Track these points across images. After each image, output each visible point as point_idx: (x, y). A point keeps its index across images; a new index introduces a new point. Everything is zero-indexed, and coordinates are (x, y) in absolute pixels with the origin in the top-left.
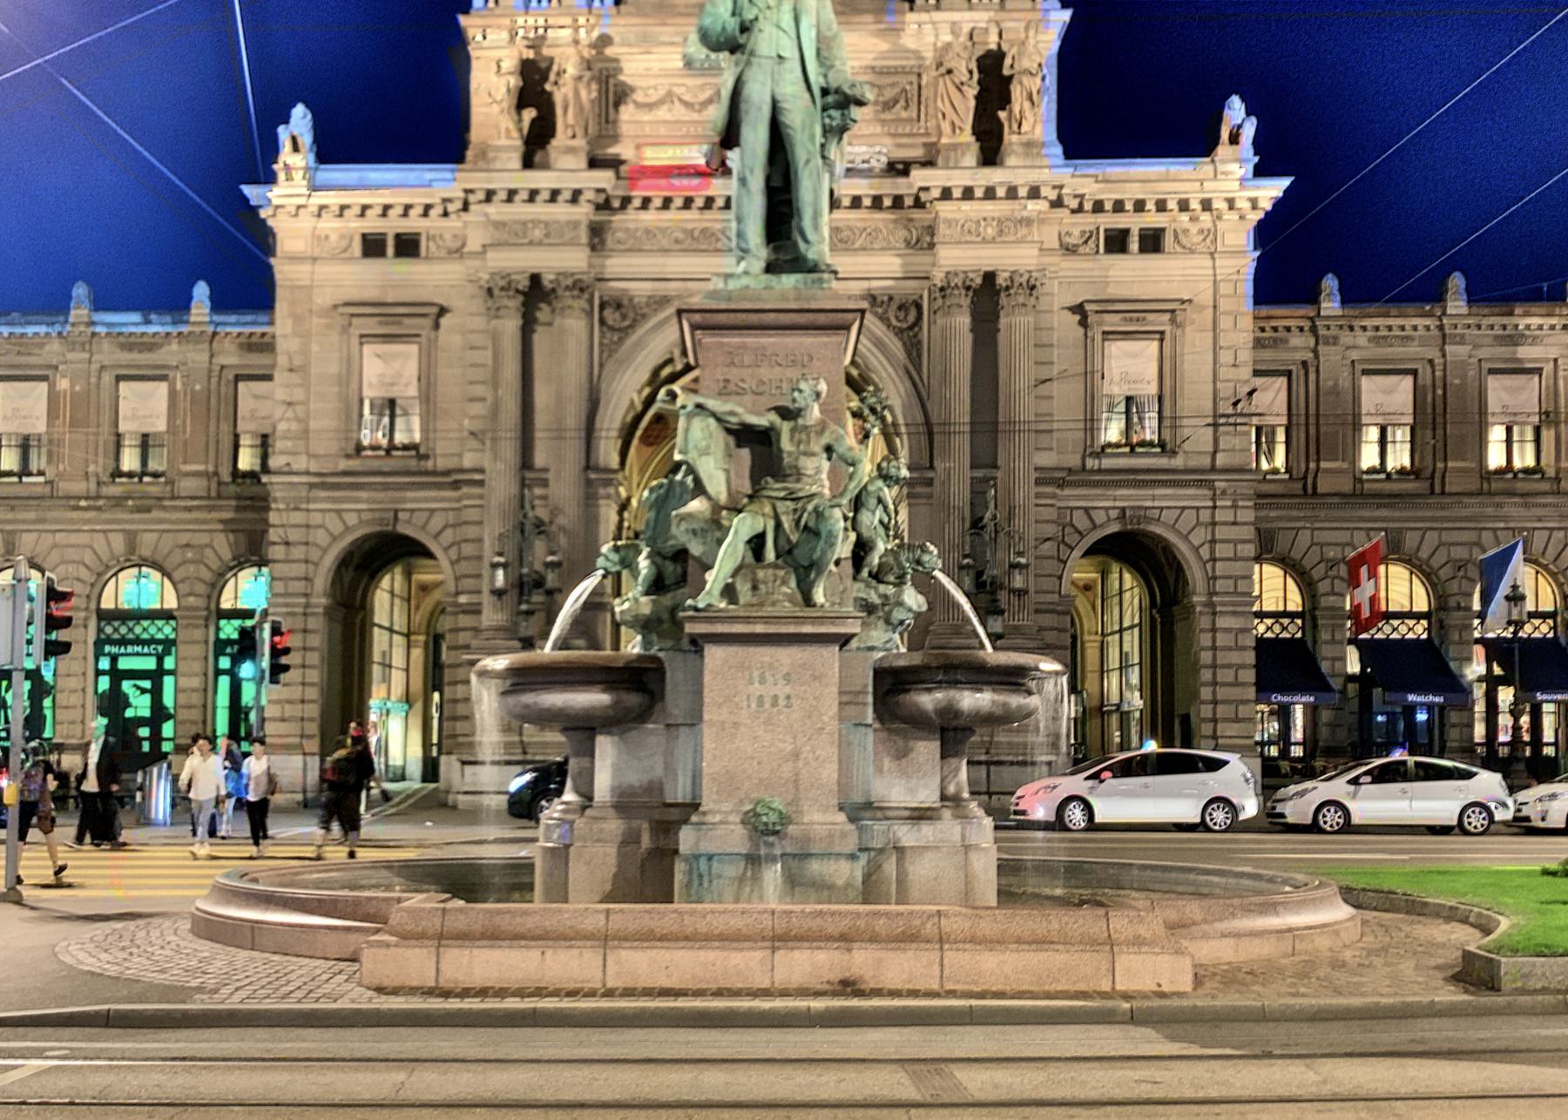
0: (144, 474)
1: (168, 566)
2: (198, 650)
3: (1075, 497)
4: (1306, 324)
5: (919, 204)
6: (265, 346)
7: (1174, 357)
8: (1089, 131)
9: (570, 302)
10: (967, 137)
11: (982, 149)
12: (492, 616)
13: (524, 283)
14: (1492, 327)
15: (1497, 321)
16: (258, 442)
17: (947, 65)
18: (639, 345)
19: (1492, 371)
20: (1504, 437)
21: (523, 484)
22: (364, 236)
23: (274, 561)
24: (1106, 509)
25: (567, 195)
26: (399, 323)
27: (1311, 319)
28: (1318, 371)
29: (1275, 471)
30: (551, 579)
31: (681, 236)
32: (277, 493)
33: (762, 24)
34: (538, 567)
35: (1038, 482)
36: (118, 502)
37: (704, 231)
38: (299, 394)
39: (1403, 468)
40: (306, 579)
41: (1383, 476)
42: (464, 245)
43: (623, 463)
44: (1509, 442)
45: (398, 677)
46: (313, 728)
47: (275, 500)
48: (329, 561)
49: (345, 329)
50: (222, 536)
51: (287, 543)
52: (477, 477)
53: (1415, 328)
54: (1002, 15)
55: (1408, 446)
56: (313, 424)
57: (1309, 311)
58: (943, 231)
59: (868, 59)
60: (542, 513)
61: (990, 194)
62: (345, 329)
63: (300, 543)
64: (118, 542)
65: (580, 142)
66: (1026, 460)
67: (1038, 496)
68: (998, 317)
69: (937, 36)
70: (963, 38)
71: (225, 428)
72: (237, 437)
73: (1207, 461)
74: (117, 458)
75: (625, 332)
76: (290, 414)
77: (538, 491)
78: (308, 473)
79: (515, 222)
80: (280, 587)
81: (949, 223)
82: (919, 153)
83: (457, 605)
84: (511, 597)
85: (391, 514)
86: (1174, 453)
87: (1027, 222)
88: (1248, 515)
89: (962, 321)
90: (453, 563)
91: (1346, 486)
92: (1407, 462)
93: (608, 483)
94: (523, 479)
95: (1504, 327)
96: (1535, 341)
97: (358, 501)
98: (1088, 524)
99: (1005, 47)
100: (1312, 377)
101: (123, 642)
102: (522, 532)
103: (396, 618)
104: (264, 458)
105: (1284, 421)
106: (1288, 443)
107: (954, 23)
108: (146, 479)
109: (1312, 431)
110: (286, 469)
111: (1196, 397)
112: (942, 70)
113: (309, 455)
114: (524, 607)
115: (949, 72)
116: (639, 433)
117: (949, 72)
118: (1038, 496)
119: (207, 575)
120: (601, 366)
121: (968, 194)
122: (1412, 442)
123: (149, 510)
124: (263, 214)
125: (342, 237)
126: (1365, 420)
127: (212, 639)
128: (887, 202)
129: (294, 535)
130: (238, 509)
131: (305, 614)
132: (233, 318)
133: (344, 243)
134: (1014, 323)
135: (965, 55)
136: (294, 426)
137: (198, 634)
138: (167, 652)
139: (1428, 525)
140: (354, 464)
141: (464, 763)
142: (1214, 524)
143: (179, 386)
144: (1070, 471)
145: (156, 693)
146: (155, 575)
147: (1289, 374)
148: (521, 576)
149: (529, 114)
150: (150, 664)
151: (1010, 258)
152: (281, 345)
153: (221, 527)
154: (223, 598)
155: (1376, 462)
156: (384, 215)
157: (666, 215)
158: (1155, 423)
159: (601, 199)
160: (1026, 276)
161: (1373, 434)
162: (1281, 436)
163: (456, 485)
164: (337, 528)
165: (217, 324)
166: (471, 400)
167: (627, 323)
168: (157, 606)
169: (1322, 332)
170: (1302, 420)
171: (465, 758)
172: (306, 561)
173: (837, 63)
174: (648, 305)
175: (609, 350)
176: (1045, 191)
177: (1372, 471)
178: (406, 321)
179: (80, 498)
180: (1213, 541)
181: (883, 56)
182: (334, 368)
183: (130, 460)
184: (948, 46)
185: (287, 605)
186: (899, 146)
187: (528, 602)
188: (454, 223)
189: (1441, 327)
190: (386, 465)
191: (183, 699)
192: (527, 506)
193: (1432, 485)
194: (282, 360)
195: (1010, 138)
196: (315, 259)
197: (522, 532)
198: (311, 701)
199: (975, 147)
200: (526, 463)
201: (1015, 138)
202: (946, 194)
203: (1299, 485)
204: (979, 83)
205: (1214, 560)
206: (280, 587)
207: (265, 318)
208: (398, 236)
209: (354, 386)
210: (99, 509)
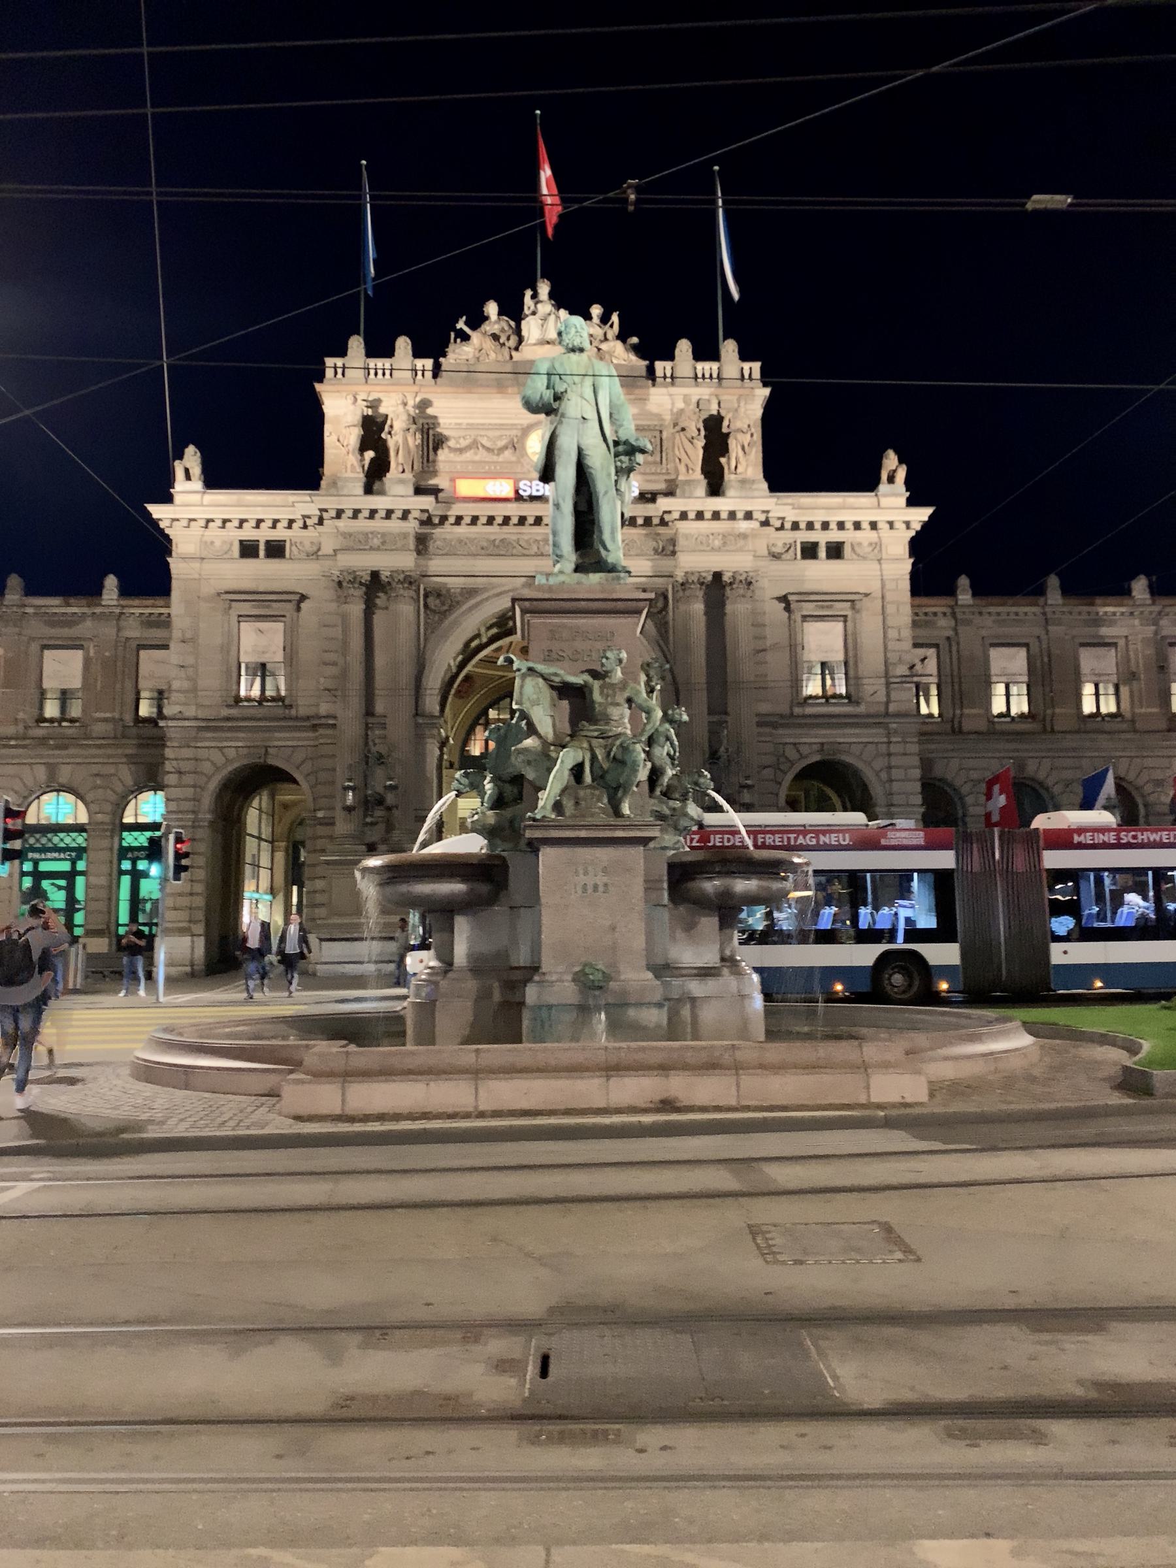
0: (63, 719)
1: (81, 791)
2: (105, 855)
3: (787, 735)
4: (948, 610)
5: (663, 523)
6: (164, 623)
7: (855, 634)
8: (784, 474)
9: (402, 592)
10: (698, 475)
11: (710, 485)
12: (343, 826)
13: (366, 578)
14: (1080, 613)
15: (1085, 609)
16: (156, 695)
17: (682, 425)
18: (456, 623)
19: (1083, 645)
20: (1093, 691)
21: (367, 727)
22: (241, 541)
23: (167, 786)
24: (810, 745)
25: (399, 514)
26: (268, 607)
27: (952, 607)
28: (958, 644)
29: (930, 716)
30: (390, 799)
31: (485, 544)
32: (171, 734)
33: (570, 395)
34: (380, 789)
35: (760, 724)
36: (43, 741)
37: (502, 541)
38: (191, 660)
39: (1023, 714)
40: (194, 800)
41: (1008, 719)
42: (319, 550)
43: (442, 710)
44: (1097, 694)
45: (264, 875)
46: (200, 915)
47: (170, 739)
48: (213, 785)
50: (125, 767)
51: (180, 773)
52: (331, 722)
53: (1026, 614)
54: (720, 391)
55: (1025, 698)
56: (202, 683)
57: (949, 601)
58: (681, 543)
60: (383, 749)
61: (716, 516)
63: (189, 773)
64: (41, 773)
65: (408, 475)
66: (746, 710)
67: (760, 735)
68: (723, 605)
69: (673, 404)
70: (693, 406)
71: (129, 685)
72: (138, 693)
73: (882, 709)
74: (41, 708)
75: (444, 614)
76: (182, 674)
77: (377, 732)
78: (196, 719)
79: (359, 533)
80: (173, 806)
81: (687, 536)
82: (661, 486)
83: (315, 818)
84: (359, 812)
85: (263, 750)
86: (858, 703)
87: (744, 536)
88: (914, 748)
89: (698, 608)
90: (312, 787)
91: (982, 726)
92: (1025, 709)
93: (434, 726)
94: (367, 724)
95: (1089, 613)
96: (1112, 623)
97: (237, 739)
98: (797, 756)
99: (723, 413)
100: (954, 648)
101: (44, 850)
102: (367, 763)
103: (263, 830)
104: (160, 708)
105: (936, 680)
106: (939, 695)
107: (685, 396)
108: (64, 724)
109: (956, 687)
110: (179, 716)
111: (871, 661)
112: (678, 428)
113: (199, 706)
114: (369, 820)
115: (683, 429)
116: (453, 691)
117: (683, 429)
118: (760, 735)
119: (113, 797)
120: (426, 640)
121: (700, 516)
122: (1028, 694)
123: (65, 747)
124: (162, 525)
125: (224, 542)
126: (994, 679)
127: (116, 846)
128: (640, 521)
129: (186, 766)
130: (140, 746)
131: (193, 827)
132: (137, 602)
133: (226, 547)
134: (736, 608)
135: (695, 417)
137: (105, 843)
138: (79, 858)
139: (1044, 754)
140: (234, 712)
141: (321, 940)
142: (889, 755)
143: (92, 653)
144: (782, 716)
145: (70, 889)
146: (71, 798)
147: (937, 646)
148: (366, 796)
149: (370, 454)
150: (65, 866)
151: (730, 563)
152: (177, 623)
153: (124, 760)
154: (126, 813)
155: (1004, 709)
156: (258, 527)
157: (473, 529)
158: (844, 682)
159: (425, 516)
160: (744, 576)
161: (1000, 689)
162: (934, 691)
163: (315, 727)
165: (123, 607)
166: (325, 664)
167: (445, 608)
168: (71, 821)
169: (959, 616)
170: (949, 680)
171: (323, 937)
172: (194, 786)
173: (625, 423)
174: (461, 594)
175: (431, 628)
176: (755, 515)
177: (1001, 715)
178: (274, 604)
179: (11, 738)
180: (890, 767)
182: (218, 640)
183: (51, 709)
184: (682, 411)
185: (178, 820)
186: (648, 481)
187: (372, 816)
188: (311, 533)
189: (1044, 614)
190: (260, 712)
191: (92, 894)
192: (371, 743)
193: (1044, 725)
194: (176, 634)
195: (728, 477)
196: (203, 559)
197: (367, 763)
198: (198, 894)
199: (703, 483)
200: (369, 712)
201: (733, 477)
202: (684, 516)
203: (949, 726)
204: (705, 437)
205: (891, 781)
206: (173, 806)
207: (160, 601)
208: (268, 542)
209: (234, 653)
210: (24, 747)
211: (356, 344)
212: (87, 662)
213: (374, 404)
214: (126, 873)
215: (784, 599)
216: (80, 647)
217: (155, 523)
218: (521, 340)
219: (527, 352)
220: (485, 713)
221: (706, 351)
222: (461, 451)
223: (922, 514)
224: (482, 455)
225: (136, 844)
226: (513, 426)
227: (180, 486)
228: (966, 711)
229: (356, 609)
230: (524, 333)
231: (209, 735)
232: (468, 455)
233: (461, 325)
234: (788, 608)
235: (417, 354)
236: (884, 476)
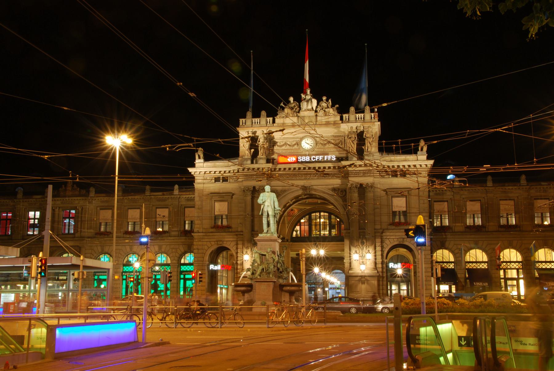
32: (195, 237)
49: (211, 199)
59: (332, 134)
62: (211, 199)
82: (344, 155)
94: (252, 234)
124: (192, 173)
134: (370, 195)
136: (199, 222)
164: (210, 245)
181: (336, 133)
194: (196, 207)
211: (249, 114)
212: (170, 212)
213: (254, 133)
214: (182, 279)
215: (385, 190)
216: (167, 208)
217: (190, 173)
218: (300, 108)
219: (302, 114)
220: (299, 221)
221: (359, 111)
222: (281, 146)
223: (431, 162)
224: (288, 147)
225: (185, 270)
226: (297, 138)
227: (197, 161)
228: (457, 224)
229: (249, 198)
230: (301, 106)
231: (206, 237)
232: (284, 147)
233: (282, 104)
234: (387, 194)
235: (268, 116)
236: (420, 149)
